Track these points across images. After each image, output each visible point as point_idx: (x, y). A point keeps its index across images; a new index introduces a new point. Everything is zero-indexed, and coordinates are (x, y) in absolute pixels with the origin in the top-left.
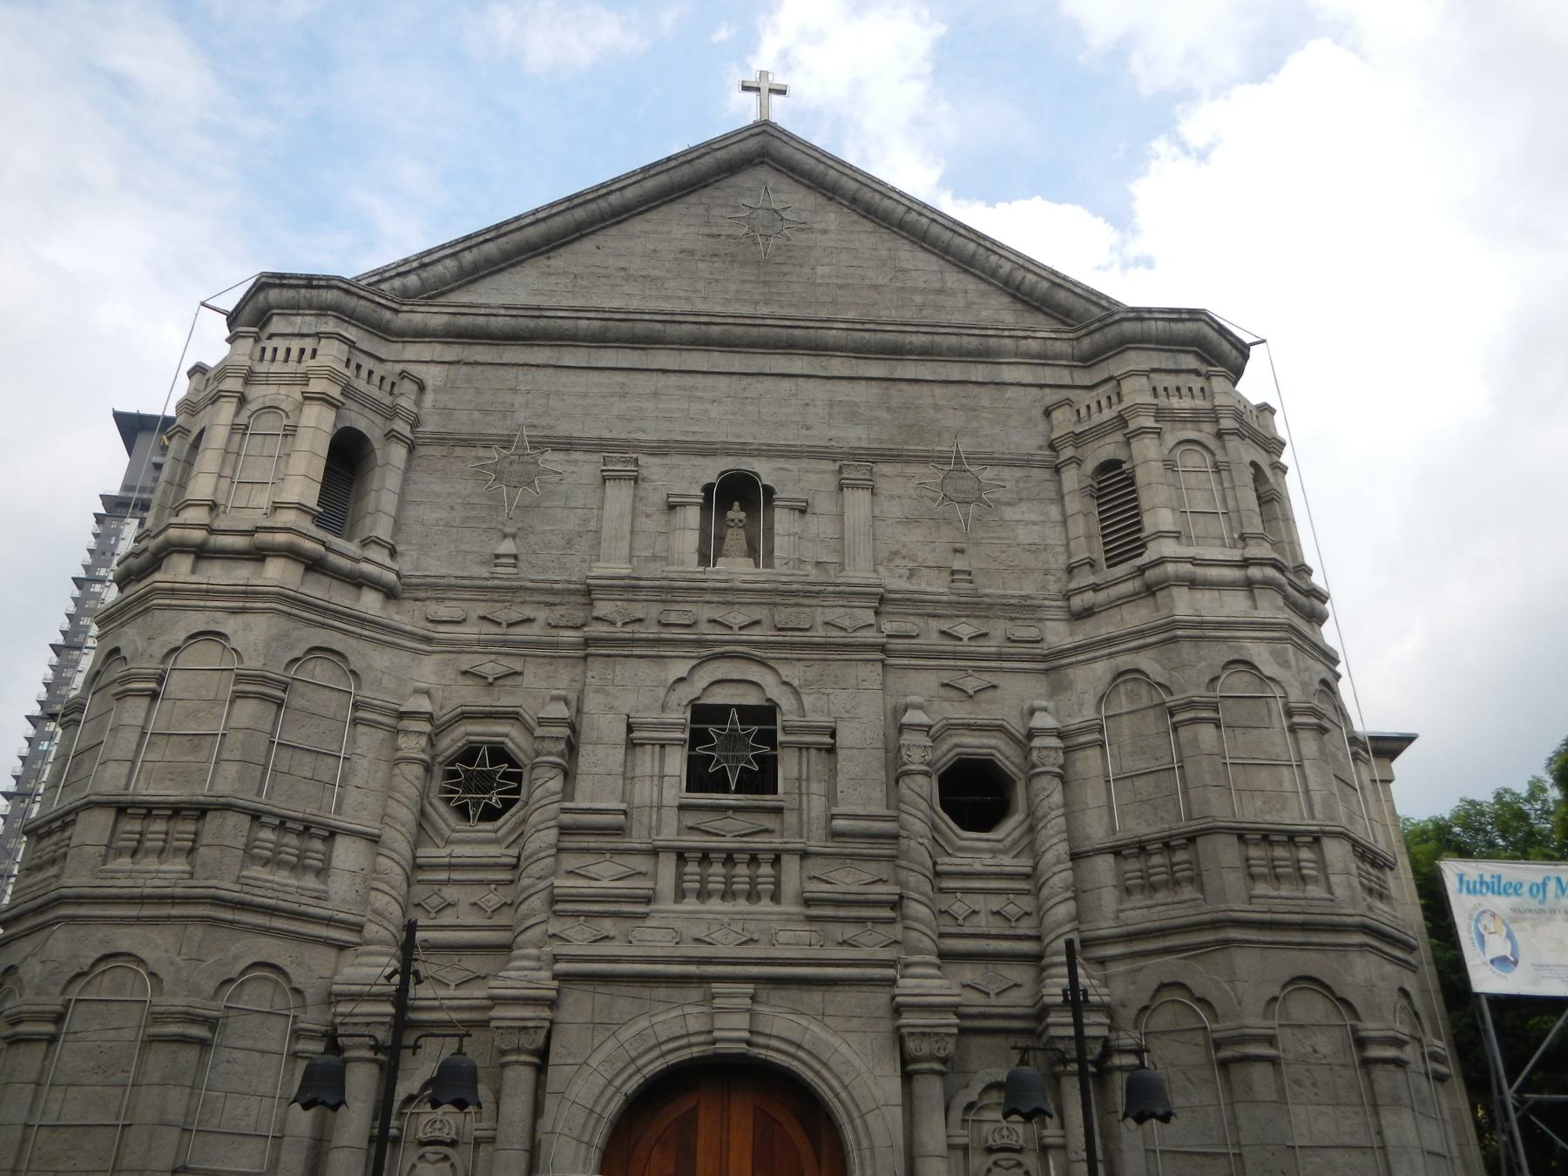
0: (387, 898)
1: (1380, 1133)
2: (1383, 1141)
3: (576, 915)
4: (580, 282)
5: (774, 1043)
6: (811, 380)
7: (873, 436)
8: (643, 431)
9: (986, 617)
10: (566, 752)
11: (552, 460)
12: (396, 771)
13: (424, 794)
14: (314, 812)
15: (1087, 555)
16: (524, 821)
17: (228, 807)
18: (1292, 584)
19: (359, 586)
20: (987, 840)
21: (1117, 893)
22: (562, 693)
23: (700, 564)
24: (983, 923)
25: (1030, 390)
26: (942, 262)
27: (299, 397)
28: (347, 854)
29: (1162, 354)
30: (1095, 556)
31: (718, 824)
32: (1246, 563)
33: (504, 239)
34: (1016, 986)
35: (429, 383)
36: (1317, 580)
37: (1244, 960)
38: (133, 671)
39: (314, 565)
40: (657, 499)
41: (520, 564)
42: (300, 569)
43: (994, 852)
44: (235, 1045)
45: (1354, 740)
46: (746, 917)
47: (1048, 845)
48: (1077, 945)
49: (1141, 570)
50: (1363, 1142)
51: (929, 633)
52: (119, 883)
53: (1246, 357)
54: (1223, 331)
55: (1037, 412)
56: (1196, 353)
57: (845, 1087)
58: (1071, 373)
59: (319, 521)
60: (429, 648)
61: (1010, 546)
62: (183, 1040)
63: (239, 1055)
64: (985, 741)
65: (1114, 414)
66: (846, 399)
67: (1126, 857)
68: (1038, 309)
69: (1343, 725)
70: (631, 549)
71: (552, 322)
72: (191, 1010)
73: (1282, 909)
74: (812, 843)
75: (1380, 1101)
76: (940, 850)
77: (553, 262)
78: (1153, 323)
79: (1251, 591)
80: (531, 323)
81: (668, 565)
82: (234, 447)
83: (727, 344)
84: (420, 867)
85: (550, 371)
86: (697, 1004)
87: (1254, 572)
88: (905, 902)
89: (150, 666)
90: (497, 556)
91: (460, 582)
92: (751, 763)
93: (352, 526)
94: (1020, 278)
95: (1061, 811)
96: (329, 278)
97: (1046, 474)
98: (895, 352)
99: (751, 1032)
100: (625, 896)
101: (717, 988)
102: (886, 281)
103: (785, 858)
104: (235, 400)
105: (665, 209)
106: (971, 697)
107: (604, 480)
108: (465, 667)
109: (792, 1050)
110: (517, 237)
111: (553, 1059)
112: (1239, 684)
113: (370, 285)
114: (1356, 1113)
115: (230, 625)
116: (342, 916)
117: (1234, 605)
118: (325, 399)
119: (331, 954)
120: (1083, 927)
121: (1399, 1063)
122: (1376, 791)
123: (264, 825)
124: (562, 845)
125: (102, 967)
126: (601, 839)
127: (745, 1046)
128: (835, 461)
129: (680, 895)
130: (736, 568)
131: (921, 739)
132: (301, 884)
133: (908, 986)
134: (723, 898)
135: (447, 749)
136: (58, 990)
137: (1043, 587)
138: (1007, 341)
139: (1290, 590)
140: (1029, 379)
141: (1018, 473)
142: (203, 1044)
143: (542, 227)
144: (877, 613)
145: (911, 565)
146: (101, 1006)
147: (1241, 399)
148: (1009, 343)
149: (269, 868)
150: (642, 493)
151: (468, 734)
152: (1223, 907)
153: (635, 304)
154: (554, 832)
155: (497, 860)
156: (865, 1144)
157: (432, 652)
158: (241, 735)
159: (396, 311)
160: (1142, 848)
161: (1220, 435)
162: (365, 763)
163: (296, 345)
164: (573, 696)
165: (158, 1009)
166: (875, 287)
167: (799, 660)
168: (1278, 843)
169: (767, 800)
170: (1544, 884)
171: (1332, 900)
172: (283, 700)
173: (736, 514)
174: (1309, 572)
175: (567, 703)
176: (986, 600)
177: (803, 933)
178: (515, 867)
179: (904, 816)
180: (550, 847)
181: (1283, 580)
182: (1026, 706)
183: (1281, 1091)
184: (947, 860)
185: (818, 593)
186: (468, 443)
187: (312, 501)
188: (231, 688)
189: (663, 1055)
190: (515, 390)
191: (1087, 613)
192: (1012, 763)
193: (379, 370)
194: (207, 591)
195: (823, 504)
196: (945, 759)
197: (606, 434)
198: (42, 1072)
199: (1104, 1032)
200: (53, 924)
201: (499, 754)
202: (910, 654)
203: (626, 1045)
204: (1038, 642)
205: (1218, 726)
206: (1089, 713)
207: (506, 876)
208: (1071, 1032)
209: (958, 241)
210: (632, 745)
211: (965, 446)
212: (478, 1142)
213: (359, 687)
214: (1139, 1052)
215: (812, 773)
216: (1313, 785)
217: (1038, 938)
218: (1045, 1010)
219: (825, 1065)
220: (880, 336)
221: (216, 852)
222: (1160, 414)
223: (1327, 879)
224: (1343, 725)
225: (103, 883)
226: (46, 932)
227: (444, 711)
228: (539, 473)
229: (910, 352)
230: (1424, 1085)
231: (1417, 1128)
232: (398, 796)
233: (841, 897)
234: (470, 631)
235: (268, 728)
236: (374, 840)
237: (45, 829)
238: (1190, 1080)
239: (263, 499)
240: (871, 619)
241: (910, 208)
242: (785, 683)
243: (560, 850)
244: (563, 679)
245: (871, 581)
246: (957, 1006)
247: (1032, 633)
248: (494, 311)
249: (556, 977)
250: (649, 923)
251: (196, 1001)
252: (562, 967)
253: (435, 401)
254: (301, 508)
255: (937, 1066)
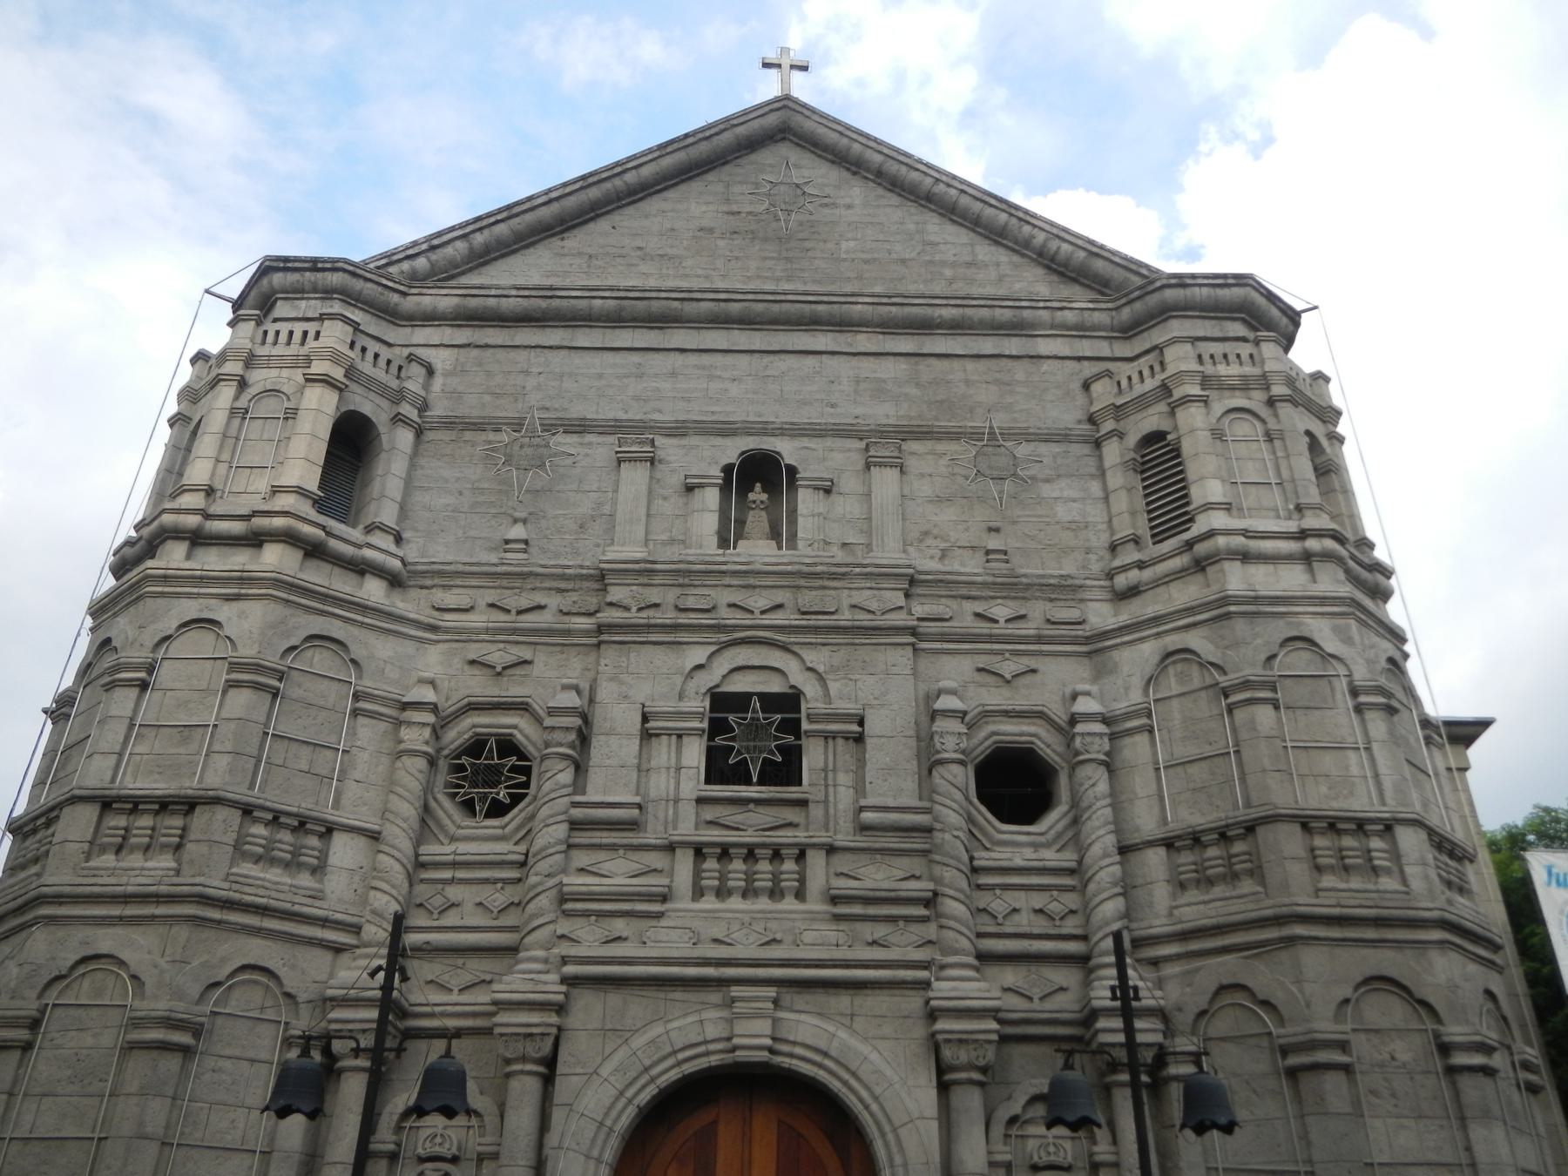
0: (387, 898)
1: (1468, 1149)
2: (1472, 1157)
3: (586, 914)
4: (595, 262)
5: (798, 1050)
6: (836, 357)
7: (901, 413)
8: (660, 411)
9: (1024, 598)
10: (577, 743)
11: (564, 442)
12: (399, 764)
13: (428, 789)
14: (309, 806)
15: (1132, 531)
16: (532, 817)
17: (217, 801)
18: (1353, 557)
20: (1028, 834)
21: (1170, 889)
22: (574, 681)
23: (720, 547)
24: (1025, 922)
25: (1068, 363)
26: (972, 234)
27: (301, 379)
28: (344, 851)
29: (1207, 323)
30: (1140, 532)
31: (739, 818)
32: (1303, 535)
33: (517, 220)
34: (1062, 989)
35: (438, 366)
36: (1380, 554)
37: (1313, 960)
38: (122, 660)
39: (314, 551)
40: (676, 480)
41: (531, 550)
42: (299, 554)
43: (1036, 846)
44: (222, 1053)
45: (1426, 723)
46: (769, 916)
47: (1093, 837)
48: (1127, 944)
49: (1189, 545)
50: (1450, 1160)
51: (963, 616)
52: (100, 881)
53: (1297, 325)
54: (1271, 297)
55: (1076, 386)
56: (1244, 321)
57: (876, 1098)
58: (1111, 344)
59: (320, 505)
60: (434, 637)
61: (1048, 524)
62: (164, 1047)
63: (227, 1064)
64: (1025, 728)
65: (1159, 384)
66: (874, 375)
67: (1179, 850)
68: (1075, 280)
69: (1413, 707)
70: (647, 533)
71: (565, 303)
72: (173, 1015)
73: (1357, 902)
74: (839, 837)
75: (1468, 1114)
76: (977, 844)
77: (566, 243)
78: (1197, 289)
79: (1310, 564)
80: (543, 304)
81: (686, 548)
82: (233, 432)
83: (747, 322)
84: (423, 866)
85: (563, 352)
86: (716, 1006)
87: (1313, 544)
88: (940, 899)
89: (140, 655)
90: (507, 542)
91: (467, 568)
92: (774, 754)
93: (358, 512)
94: (1055, 248)
95: (1108, 801)
96: (334, 260)
97: (1086, 449)
98: (924, 326)
99: (774, 1039)
100: (639, 894)
101: (736, 991)
102: (914, 255)
103: (810, 853)
104: (235, 383)
105: (683, 187)
106: (1008, 682)
107: (619, 462)
108: (472, 656)
109: (818, 1058)
110: (529, 217)
111: (561, 1069)
112: (1298, 662)
113: (378, 268)
114: (1441, 1127)
115: (223, 612)
116: (339, 916)
117: (1291, 579)
118: (327, 381)
119: (328, 956)
120: (1134, 925)
121: (1488, 1071)
122: (1453, 780)
123: (256, 820)
124: (572, 841)
125: (81, 970)
126: (614, 834)
127: (766, 1053)
128: (861, 439)
129: (698, 892)
130: (757, 550)
131: (955, 726)
132: (294, 882)
133: (944, 989)
134: (744, 895)
135: (452, 742)
136: (33, 994)
137: (1084, 567)
138: (1041, 312)
139: (1351, 564)
140: (1067, 352)
141: (1056, 448)
142: (186, 1051)
143: (555, 207)
144: (907, 596)
145: (943, 545)
146: (80, 1011)
147: (1293, 366)
148: (1045, 315)
149: (261, 864)
150: (658, 475)
151: (474, 726)
152: (1286, 901)
153: (652, 283)
154: (565, 826)
155: (503, 857)
156: (898, 1160)
157: (439, 641)
158: (232, 725)
159: (404, 294)
160: (1195, 839)
161: (1271, 402)
162: (365, 756)
163: (298, 328)
164: (585, 686)
165: (139, 1014)
166: (903, 261)
167: (824, 645)
168: (1346, 831)
169: (791, 792)
171: (1407, 893)
172: (278, 690)
173: (758, 495)
174: (1371, 546)
175: (579, 692)
176: (1024, 580)
177: (830, 932)
178: (523, 864)
179: (937, 807)
180: (559, 842)
181: (1344, 553)
182: (1068, 691)
183: (1356, 1102)
184: (984, 854)
185: (844, 574)
186: (478, 426)
187: (312, 484)
188: (225, 677)
189: (679, 1063)
190: (526, 372)
191: (1133, 592)
192: (1054, 751)
193: (385, 353)
194: (201, 578)
195: (850, 483)
196: (981, 748)
197: (621, 415)
198: (15, 1081)
199: (1158, 1038)
200: (32, 925)
201: (508, 746)
202: (943, 637)
203: (639, 1053)
204: (1080, 623)
205: (1277, 708)
206: (1136, 697)
207: (514, 874)
208: (1121, 1038)
209: (989, 211)
210: (647, 735)
211: (999, 421)
212: (481, 1158)
213: (359, 677)
214: (1196, 1058)
215: (840, 764)
216: (1382, 770)
217: (1085, 938)
218: (1095, 1014)
219: (854, 1074)
220: (907, 310)
221: (204, 849)
222: (1206, 381)
223: (1402, 872)
224: (1413, 707)
225: (85, 881)
226: (24, 934)
227: (450, 703)
228: (550, 456)
229: (939, 326)
230: (1516, 1097)
231: (1511, 1146)
232: (399, 790)
233: (871, 894)
234: (477, 620)
235: (262, 719)
236: (374, 836)
237: (31, 826)
238: (1255, 1091)
239: (262, 484)
240: (901, 601)
241: (938, 180)
242: (810, 669)
243: (570, 846)
244: (575, 667)
245: (900, 562)
246: (998, 1010)
247: (1073, 614)
248: (505, 292)
249: (565, 980)
250: (664, 923)
251: (180, 1006)
252: (570, 969)
253: (444, 385)
254: (300, 491)
255: (976, 1076)
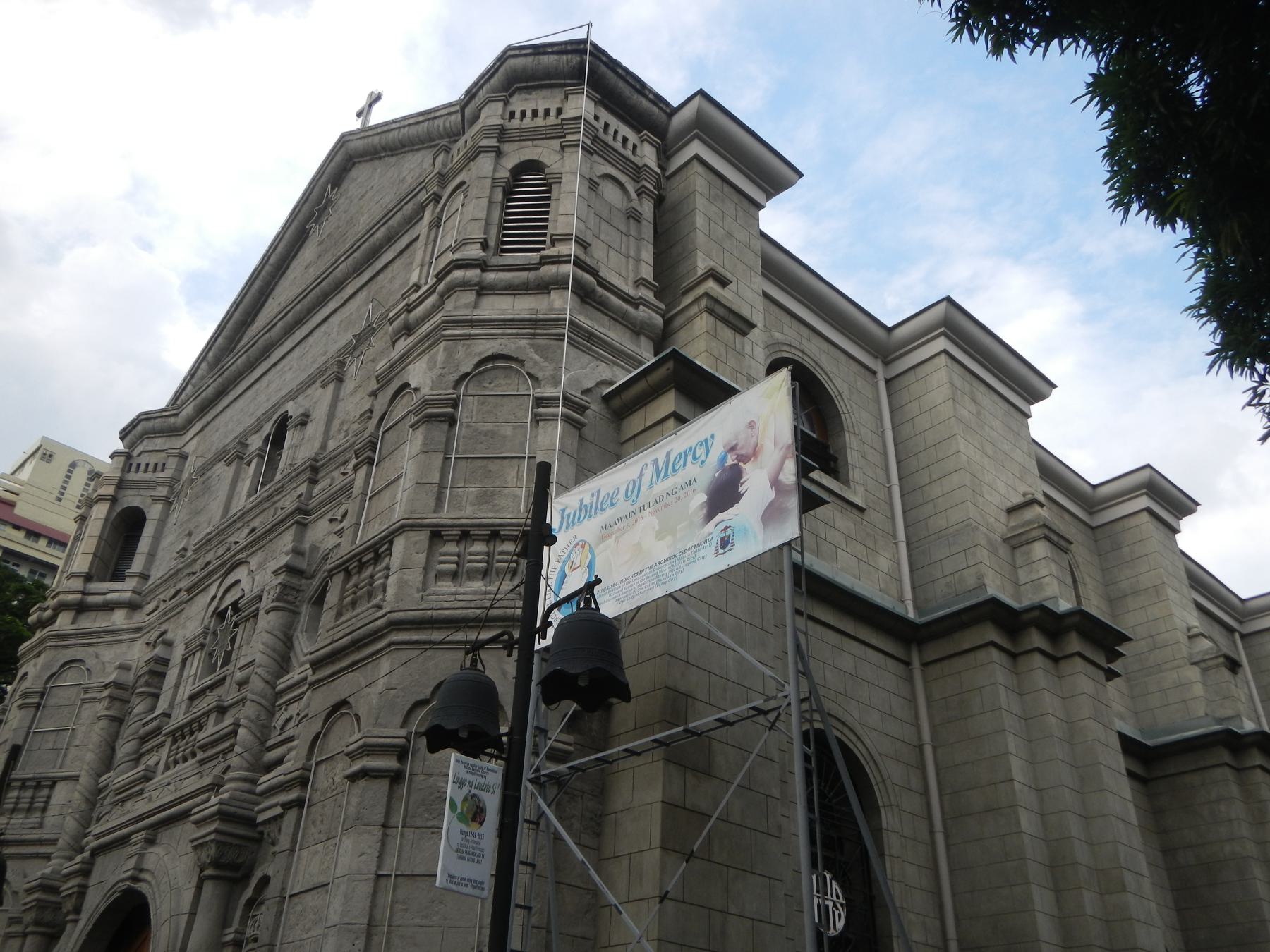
19: (112, 609)
28: (61, 794)
73: (341, 634)
78: (481, 92)
80: (220, 380)
83: (299, 322)
159: (176, 415)
162: (83, 728)
170: (641, 475)
180: (128, 754)
185: (282, 487)
